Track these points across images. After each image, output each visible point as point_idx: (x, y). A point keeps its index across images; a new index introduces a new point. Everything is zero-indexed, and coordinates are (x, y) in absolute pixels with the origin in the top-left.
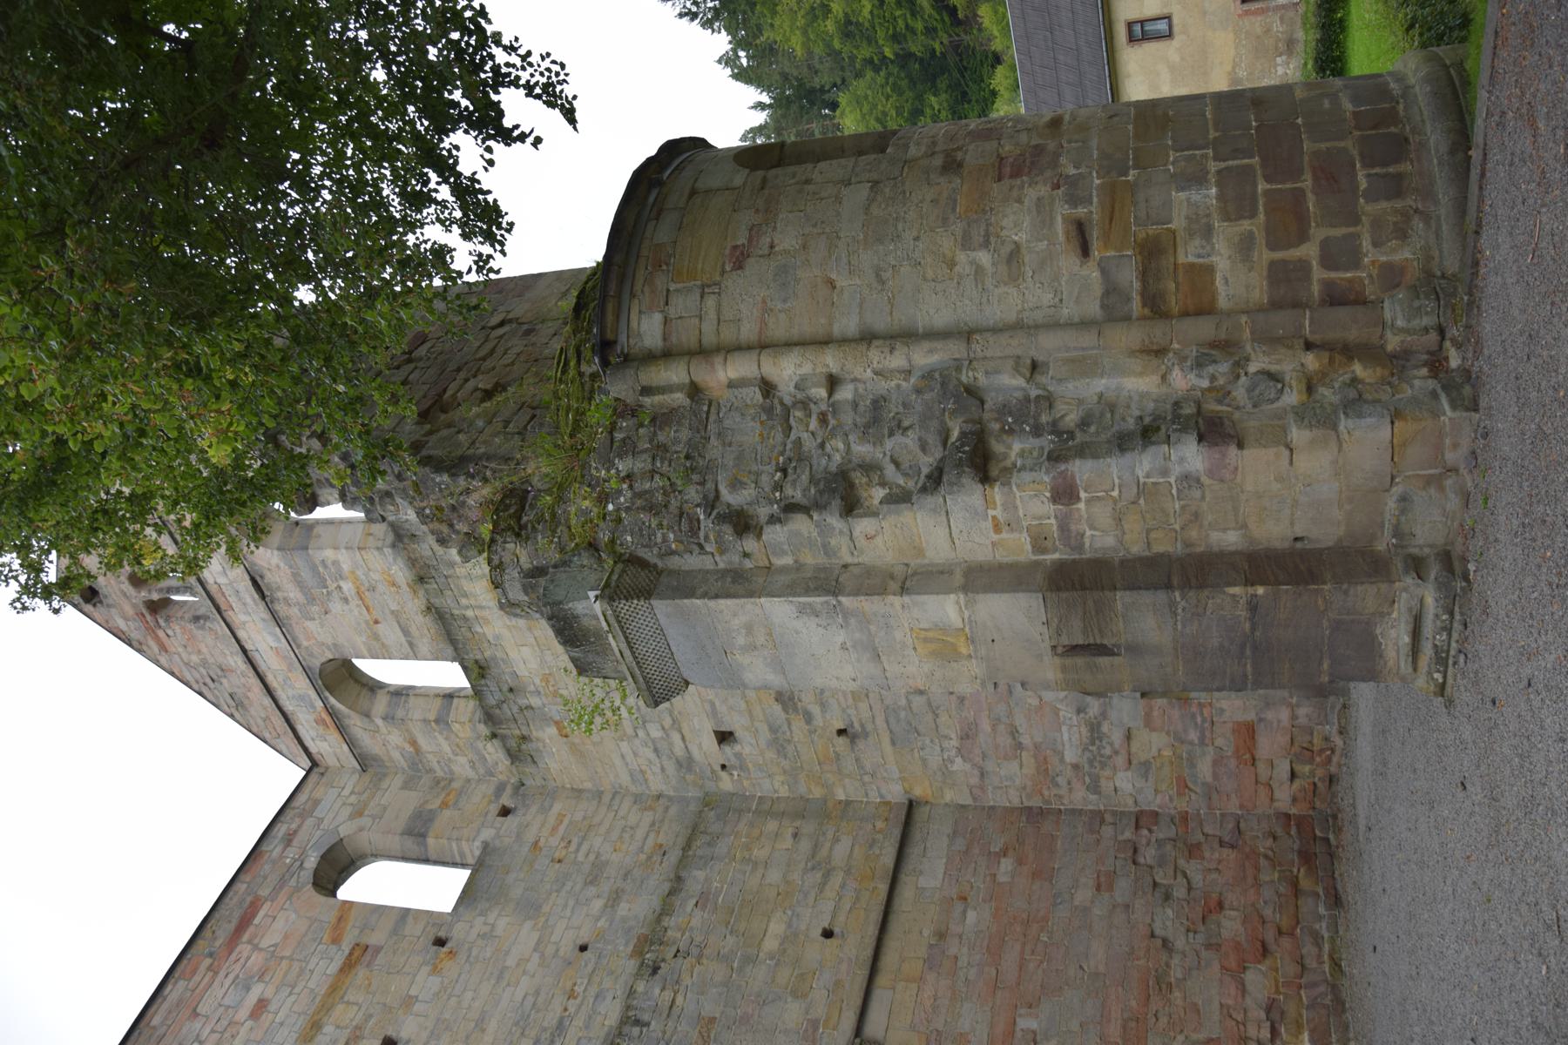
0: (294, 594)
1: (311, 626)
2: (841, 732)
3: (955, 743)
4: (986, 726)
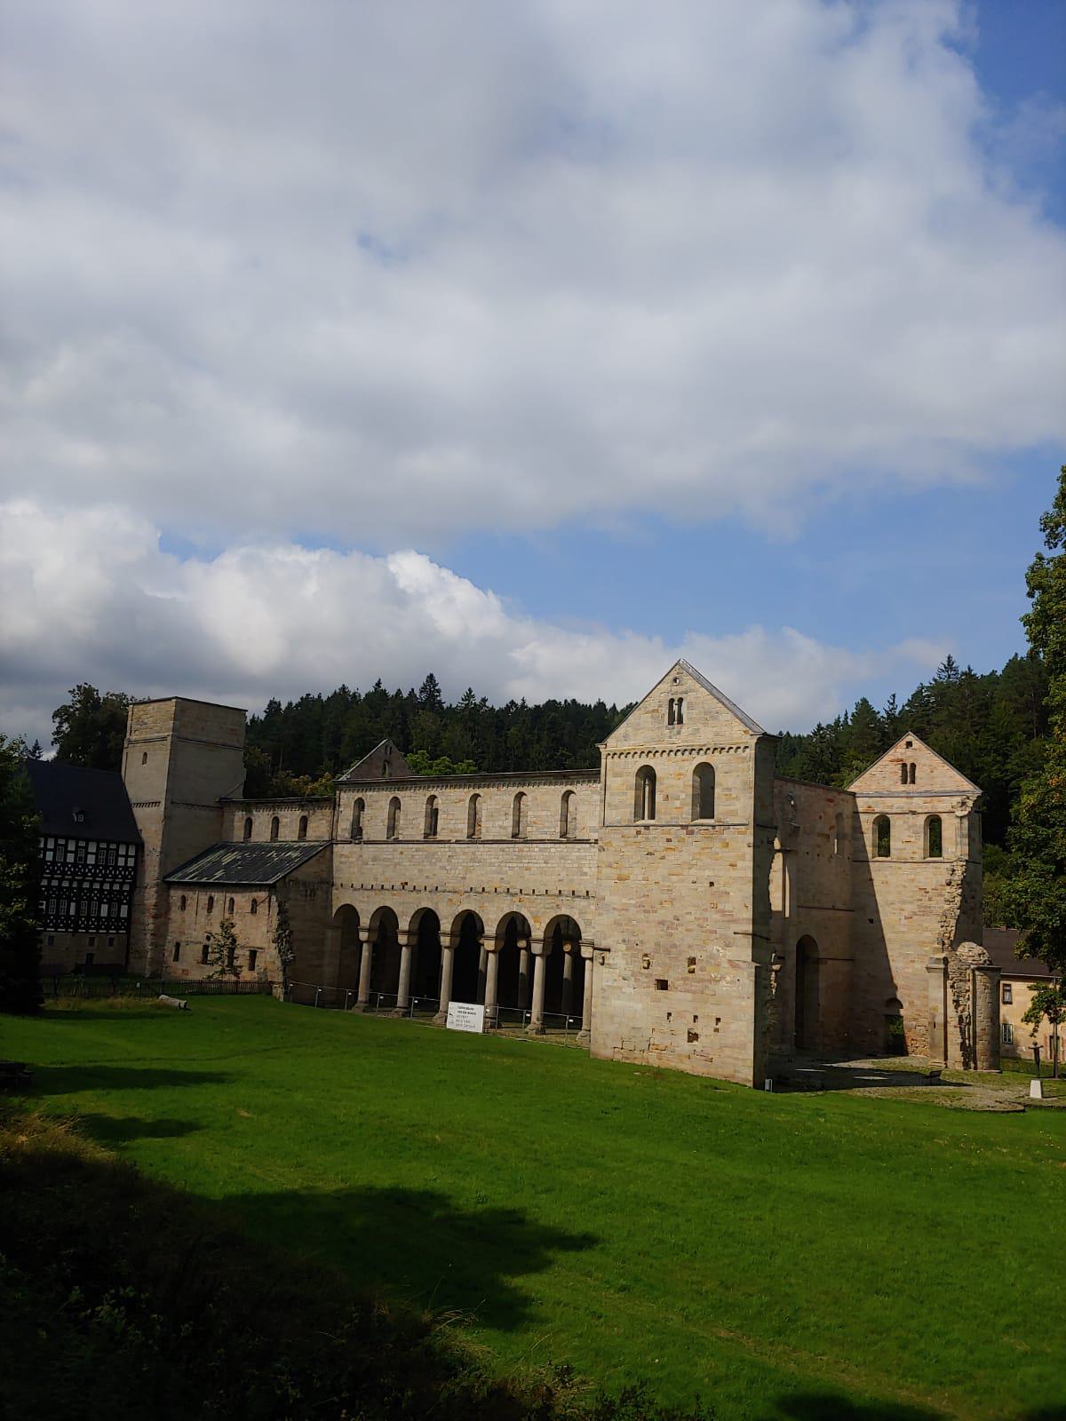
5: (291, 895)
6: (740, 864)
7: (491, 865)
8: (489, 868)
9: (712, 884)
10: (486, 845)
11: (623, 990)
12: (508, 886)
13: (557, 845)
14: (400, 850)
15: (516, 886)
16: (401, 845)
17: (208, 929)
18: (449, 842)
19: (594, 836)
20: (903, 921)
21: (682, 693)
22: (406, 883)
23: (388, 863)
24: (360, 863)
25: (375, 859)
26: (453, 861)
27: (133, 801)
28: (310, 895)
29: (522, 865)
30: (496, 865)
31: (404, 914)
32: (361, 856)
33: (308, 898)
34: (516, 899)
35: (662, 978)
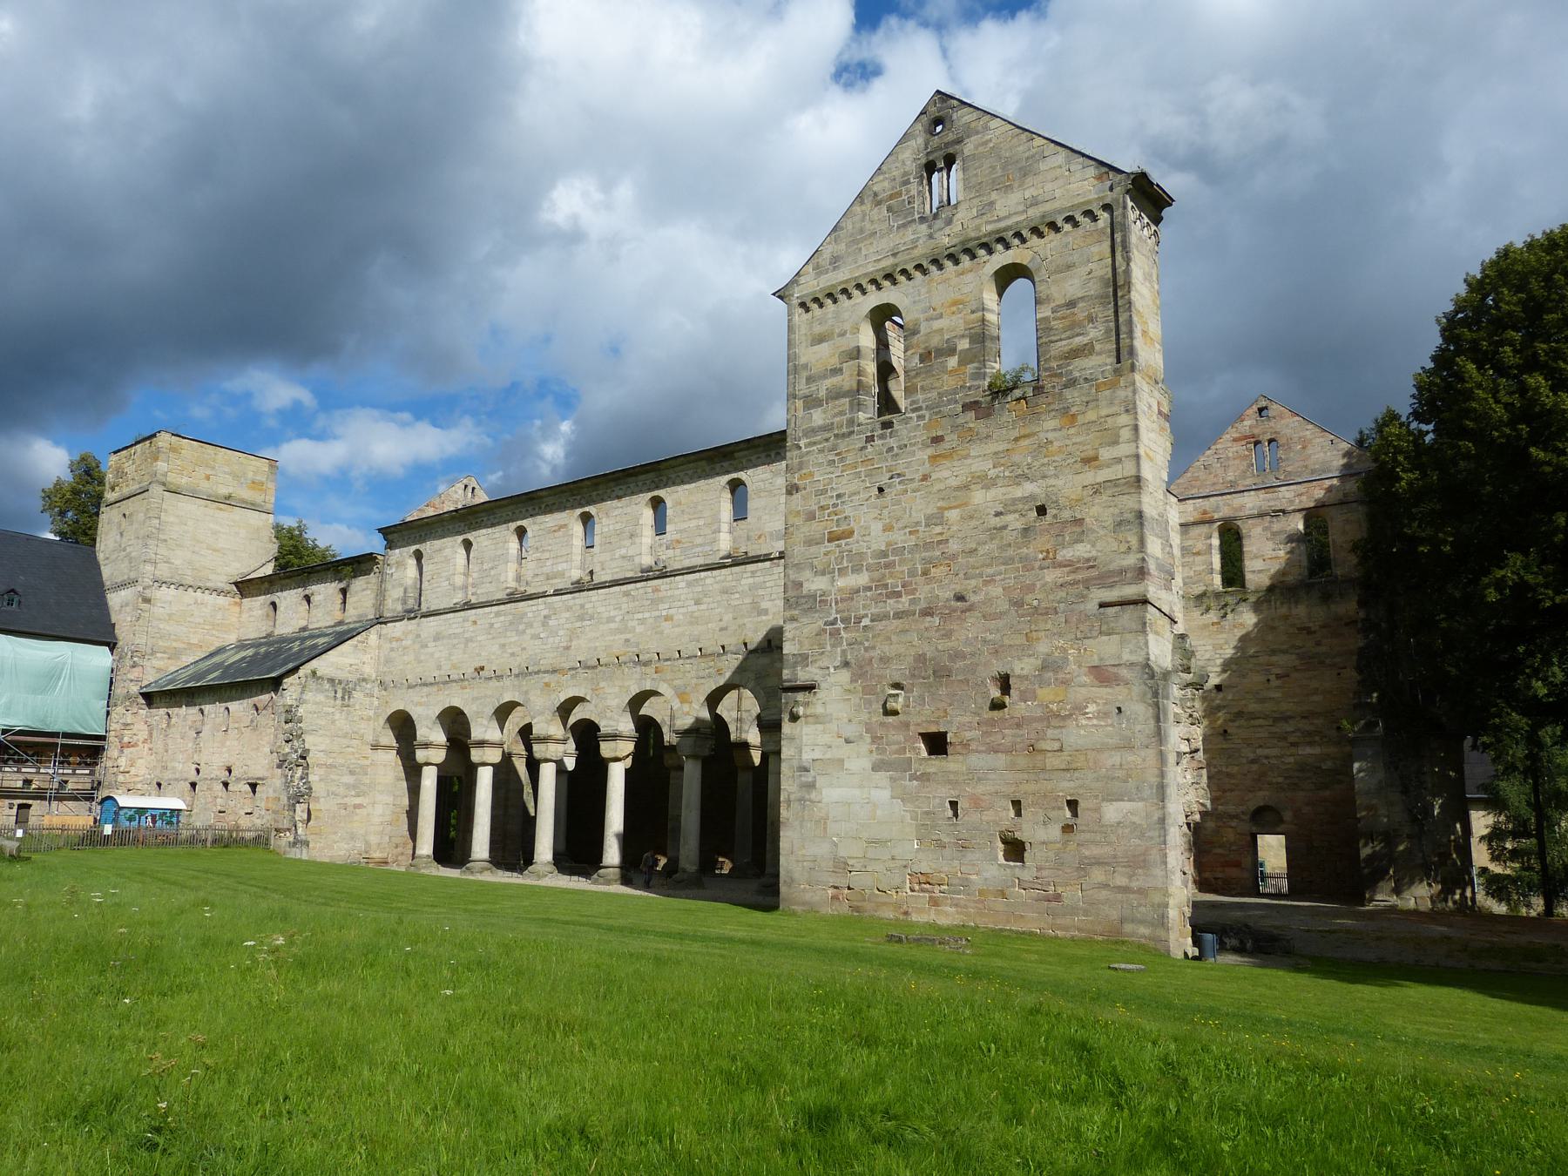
0: (1276, 527)
1: (1259, 530)
2: (1225, 731)
3: (1224, 769)
4: (1233, 781)
5: (308, 696)
6: (1106, 454)
7: (610, 620)
8: (605, 627)
9: (1042, 510)
10: (600, 591)
11: (846, 765)
12: (636, 650)
13: (715, 573)
14: (473, 618)
15: (651, 646)
16: (473, 611)
17: (196, 759)
18: (544, 595)
19: (779, 546)
20: (1275, 683)
21: (947, 145)
22: (482, 668)
23: (455, 641)
24: (417, 646)
25: (437, 638)
26: (551, 623)
27: (108, 584)
28: (343, 698)
29: (657, 613)
30: (617, 619)
31: (478, 714)
32: (418, 636)
33: (339, 702)
34: (650, 670)
35: (933, 729)
